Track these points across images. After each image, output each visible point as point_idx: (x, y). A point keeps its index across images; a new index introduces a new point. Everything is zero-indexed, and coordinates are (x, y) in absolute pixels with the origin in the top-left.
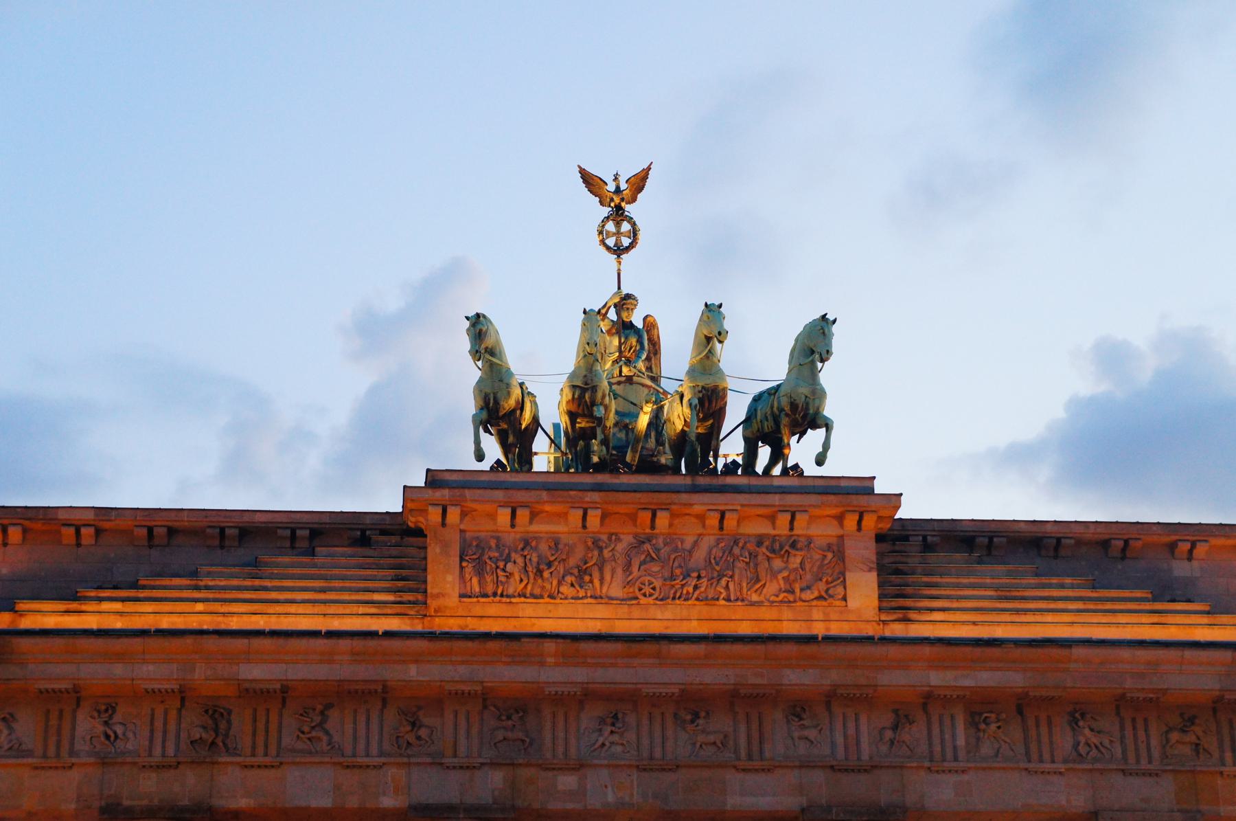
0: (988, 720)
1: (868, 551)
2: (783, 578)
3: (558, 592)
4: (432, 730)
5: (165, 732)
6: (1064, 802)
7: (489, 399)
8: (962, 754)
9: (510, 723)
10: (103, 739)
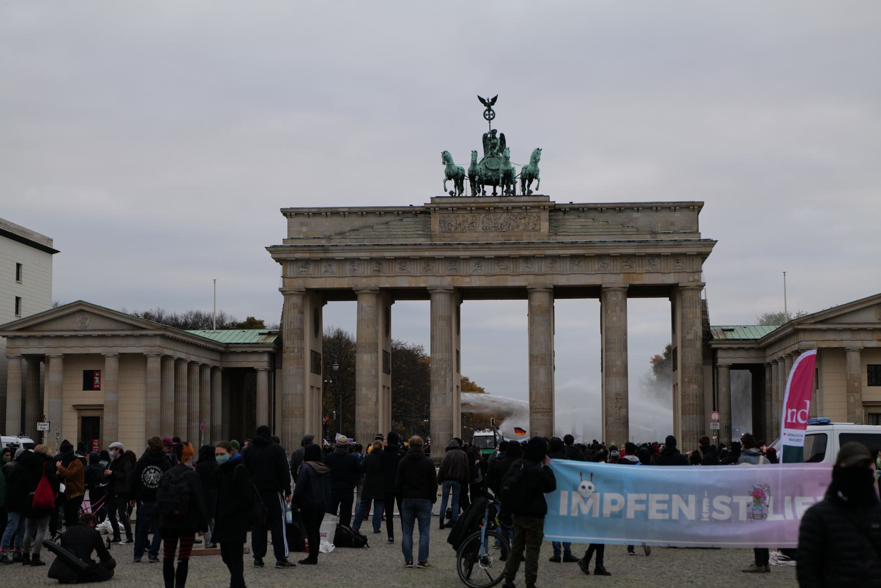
4: (433, 267)
5: (367, 269)
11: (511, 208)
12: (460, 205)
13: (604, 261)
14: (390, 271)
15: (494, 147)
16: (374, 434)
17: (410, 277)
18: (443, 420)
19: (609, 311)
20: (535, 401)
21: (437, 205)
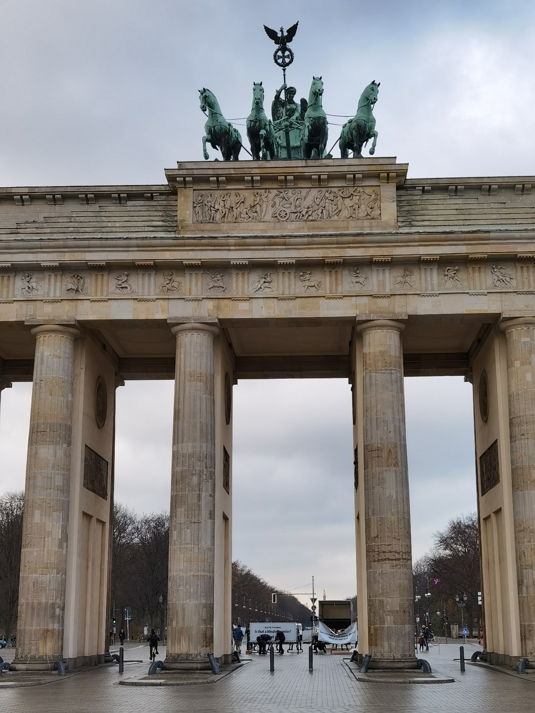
0: (450, 271)
1: (392, 193)
2: (350, 207)
3: (240, 217)
5: (55, 286)
6: (486, 308)
7: (212, 130)
8: (436, 288)
9: (216, 279)
10: (27, 289)
11: (326, 177)
12: (232, 171)
13: (503, 271)
14: (99, 290)
15: (291, 112)
16: (53, 604)
17: (135, 301)
18: (193, 575)
19: (517, 364)
20: (377, 537)
21: (190, 172)
